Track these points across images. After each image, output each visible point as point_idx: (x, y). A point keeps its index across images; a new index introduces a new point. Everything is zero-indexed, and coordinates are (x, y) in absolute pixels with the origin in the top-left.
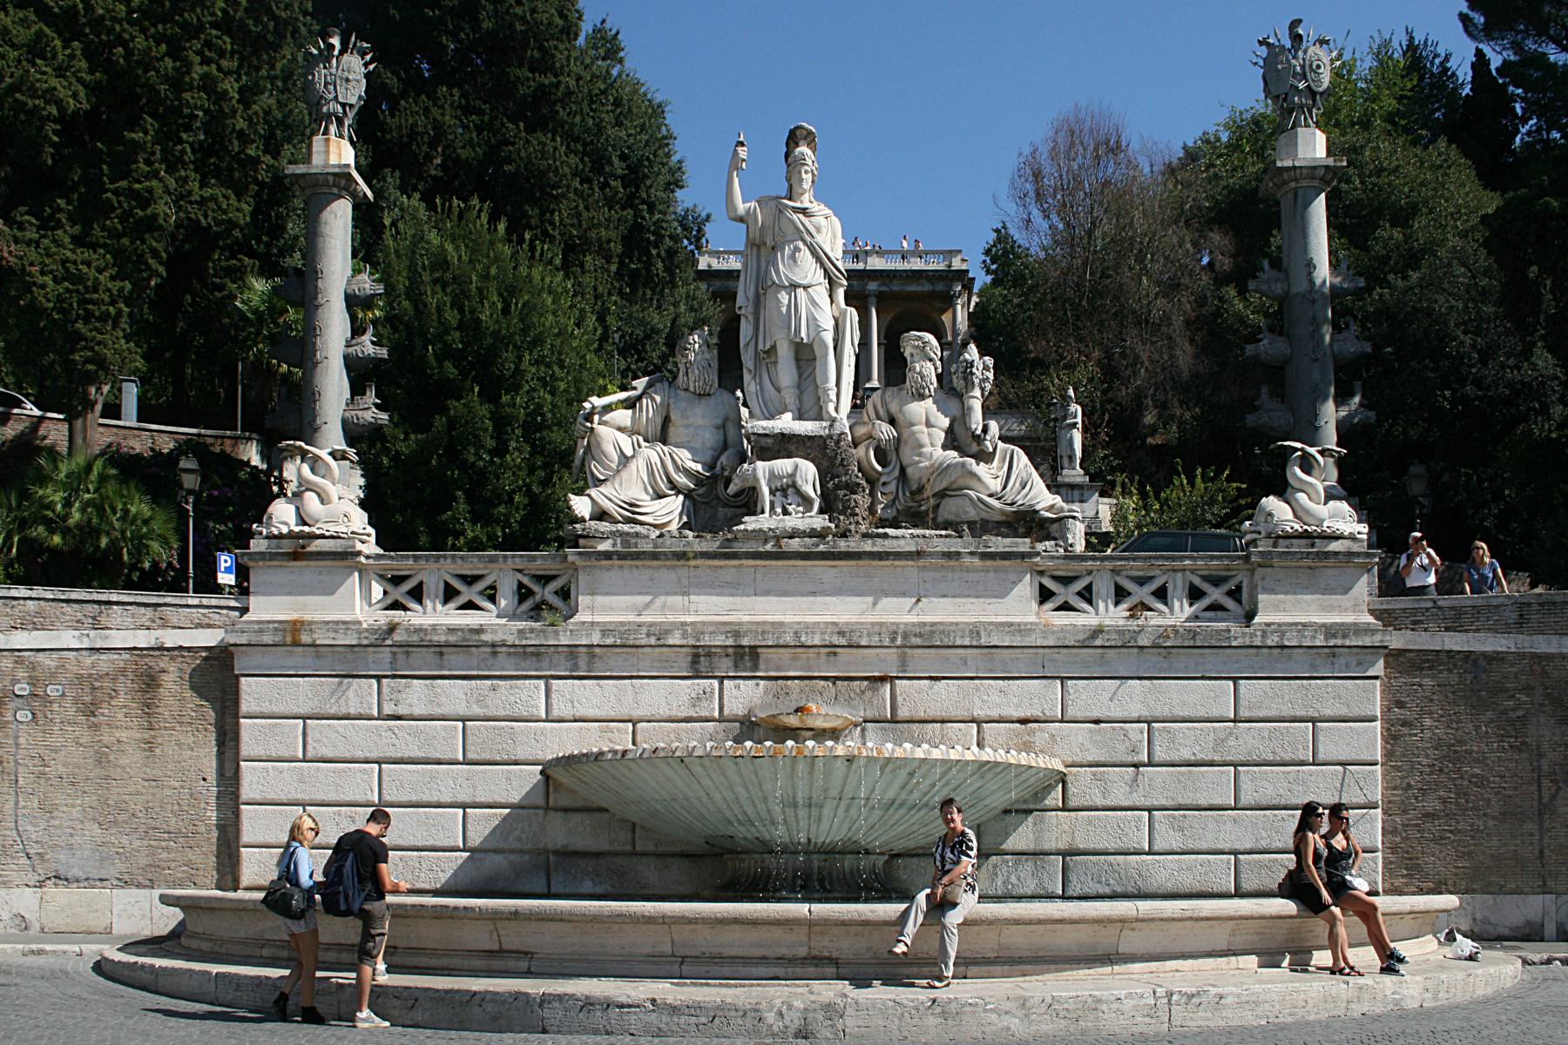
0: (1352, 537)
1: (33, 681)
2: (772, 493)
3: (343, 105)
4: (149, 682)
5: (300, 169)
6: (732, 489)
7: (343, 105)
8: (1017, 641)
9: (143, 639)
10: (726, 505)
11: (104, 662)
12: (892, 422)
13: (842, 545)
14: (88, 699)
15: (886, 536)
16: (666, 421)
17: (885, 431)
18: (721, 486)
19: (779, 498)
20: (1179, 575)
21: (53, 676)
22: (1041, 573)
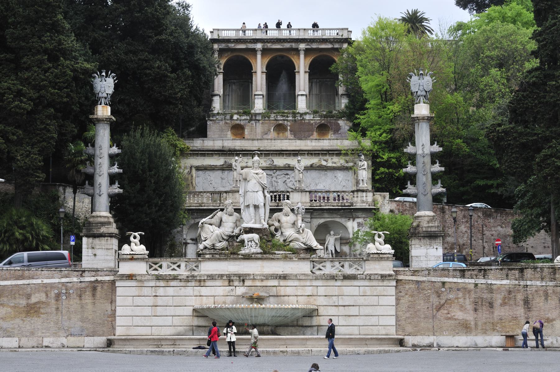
0: (389, 254)
1: (66, 290)
2: (248, 242)
3: (107, 94)
4: (94, 289)
5: (95, 117)
6: (238, 240)
7: (107, 94)
8: (306, 278)
9: (93, 279)
10: (237, 242)
11: (83, 285)
12: (279, 221)
13: (265, 256)
14: (79, 293)
15: (275, 254)
16: (221, 221)
17: (277, 224)
18: (235, 239)
19: (250, 243)
20: (347, 263)
21: (71, 288)
22: (313, 261)
